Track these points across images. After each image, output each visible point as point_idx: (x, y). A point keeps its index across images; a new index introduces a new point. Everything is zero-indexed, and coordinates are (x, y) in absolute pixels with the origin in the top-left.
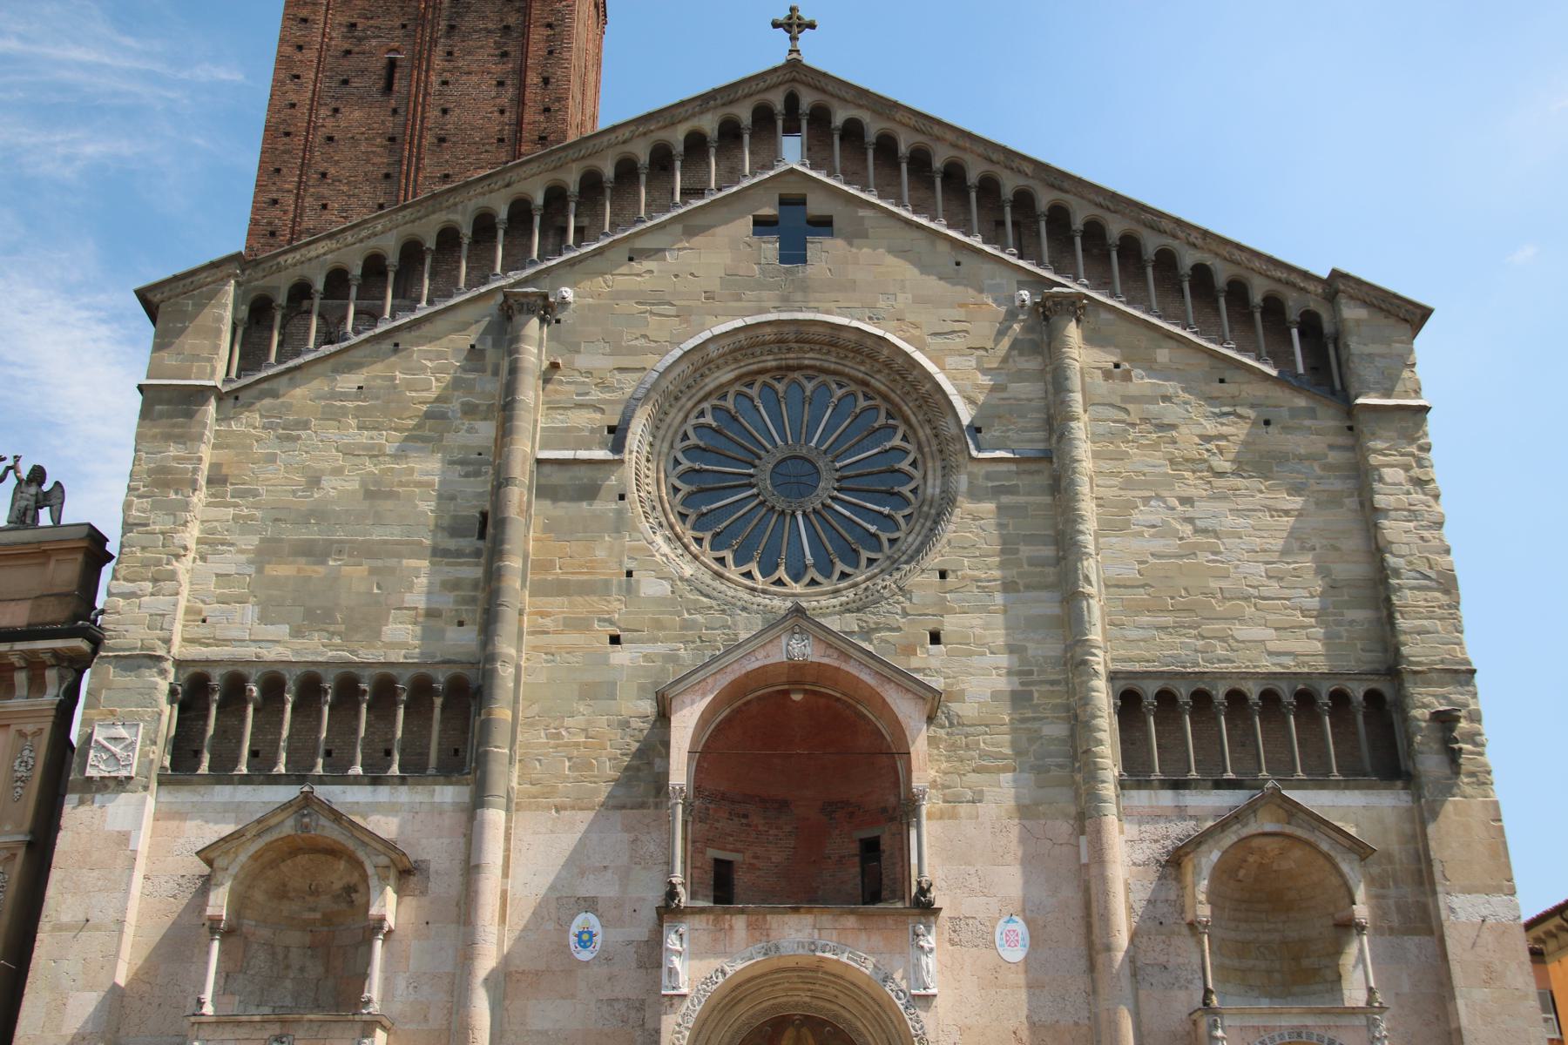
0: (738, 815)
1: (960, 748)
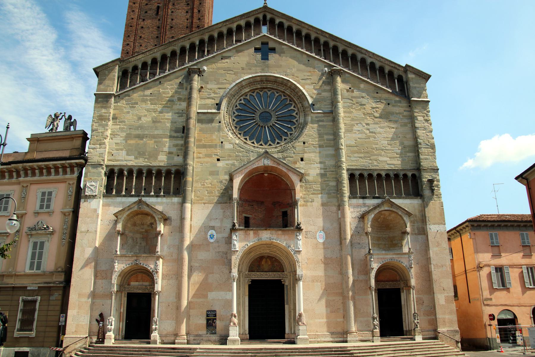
0: (251, 205)
1: (308, 188)
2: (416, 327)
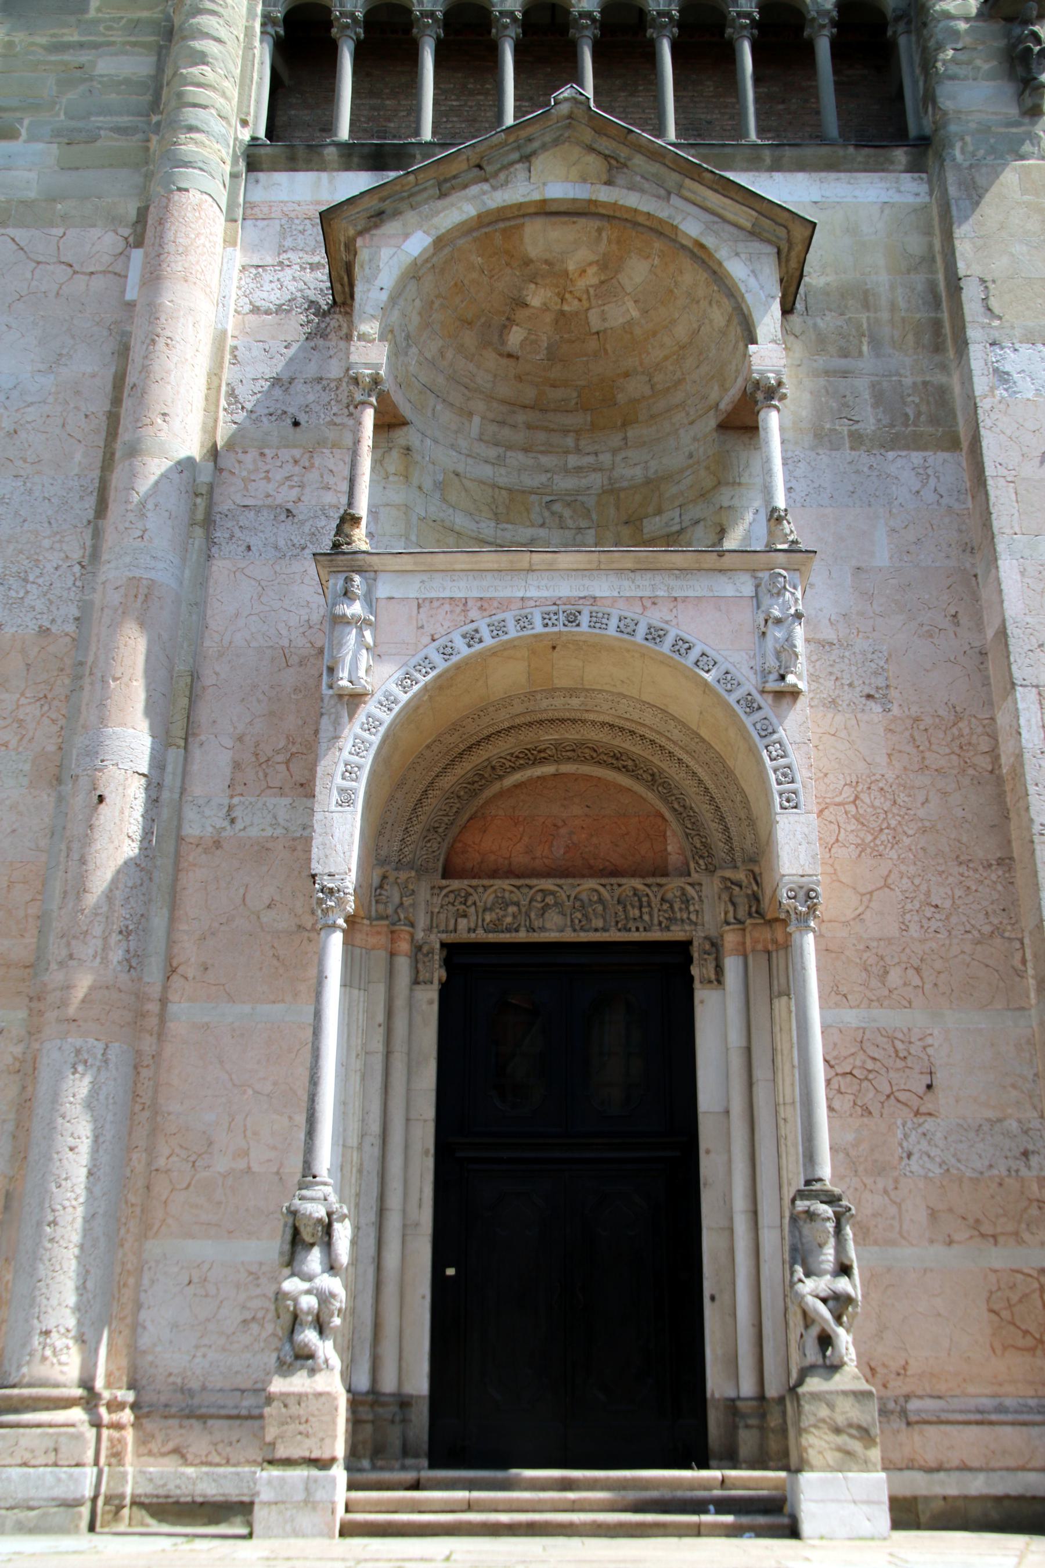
2: (813, 1356)
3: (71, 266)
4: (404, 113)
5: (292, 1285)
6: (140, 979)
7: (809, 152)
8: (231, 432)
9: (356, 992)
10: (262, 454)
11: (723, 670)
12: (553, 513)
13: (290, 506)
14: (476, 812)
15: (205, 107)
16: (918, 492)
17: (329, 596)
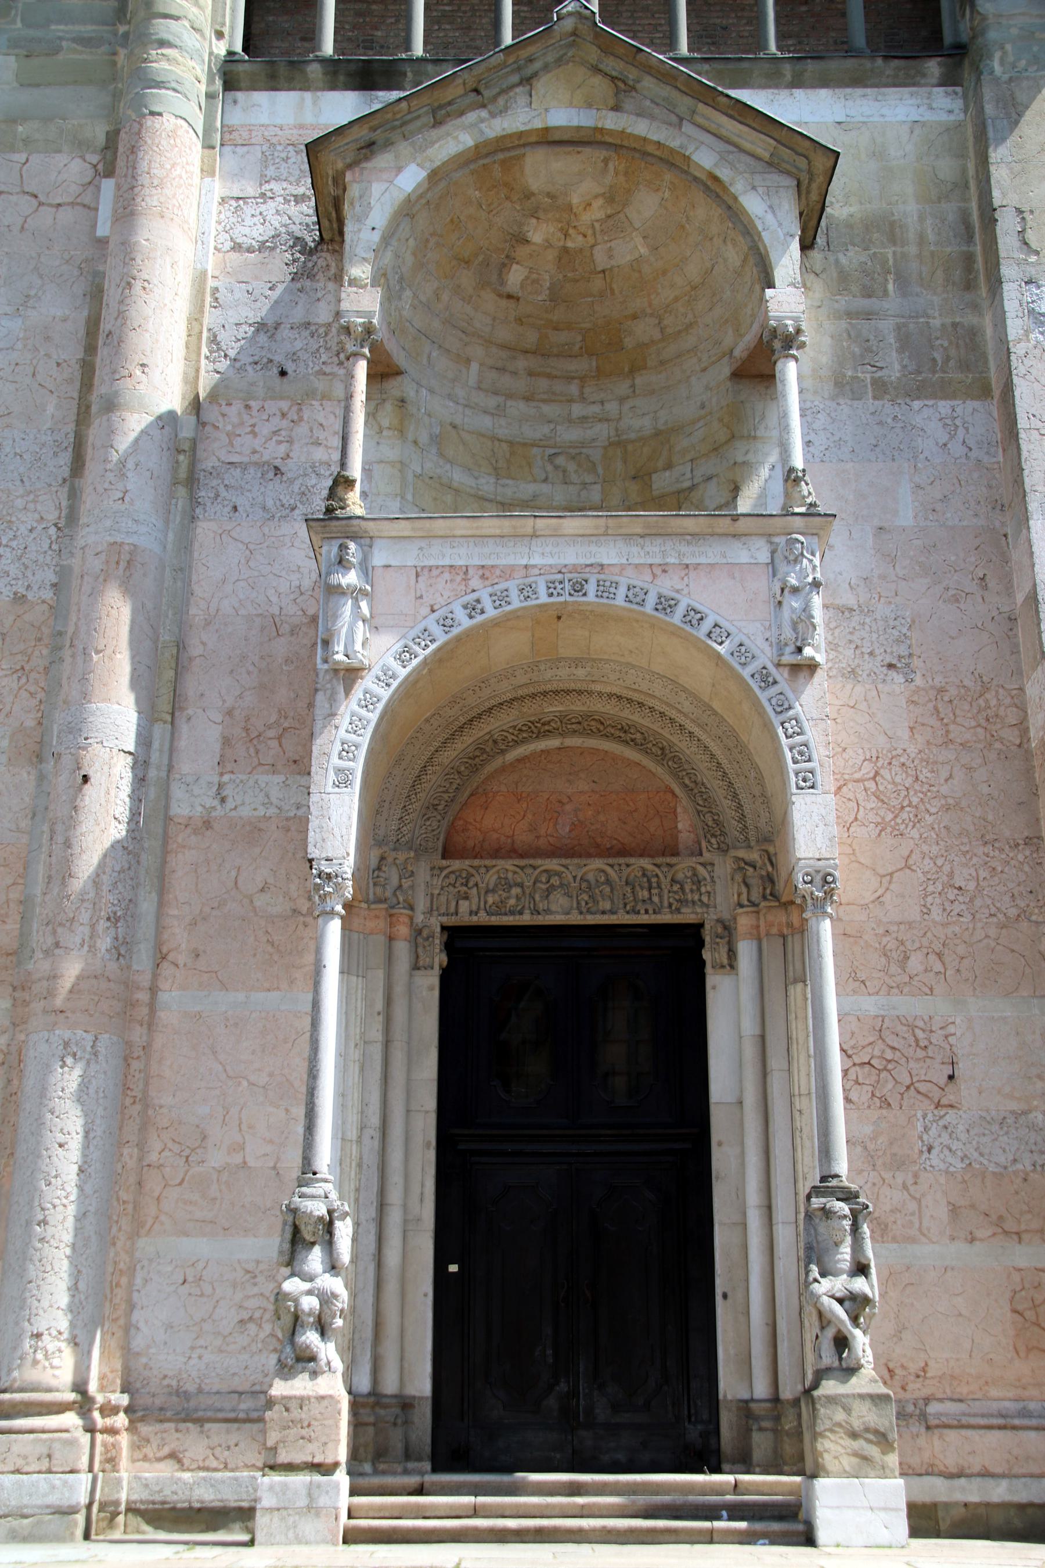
2: (828, 1358)
3: (36, 197)
4: (393, 20)
5: (293, 1285)
6: (129, 967)
7: (834, 65)
8: (213, 382)
9: (354, 978)
10: (248, 407)
11: (737, 642)
12: (556, 467)
13: (278, 462)
14: (477, 788)
15: (177, 18)
16: (945, 445)
17: (323, 560)
